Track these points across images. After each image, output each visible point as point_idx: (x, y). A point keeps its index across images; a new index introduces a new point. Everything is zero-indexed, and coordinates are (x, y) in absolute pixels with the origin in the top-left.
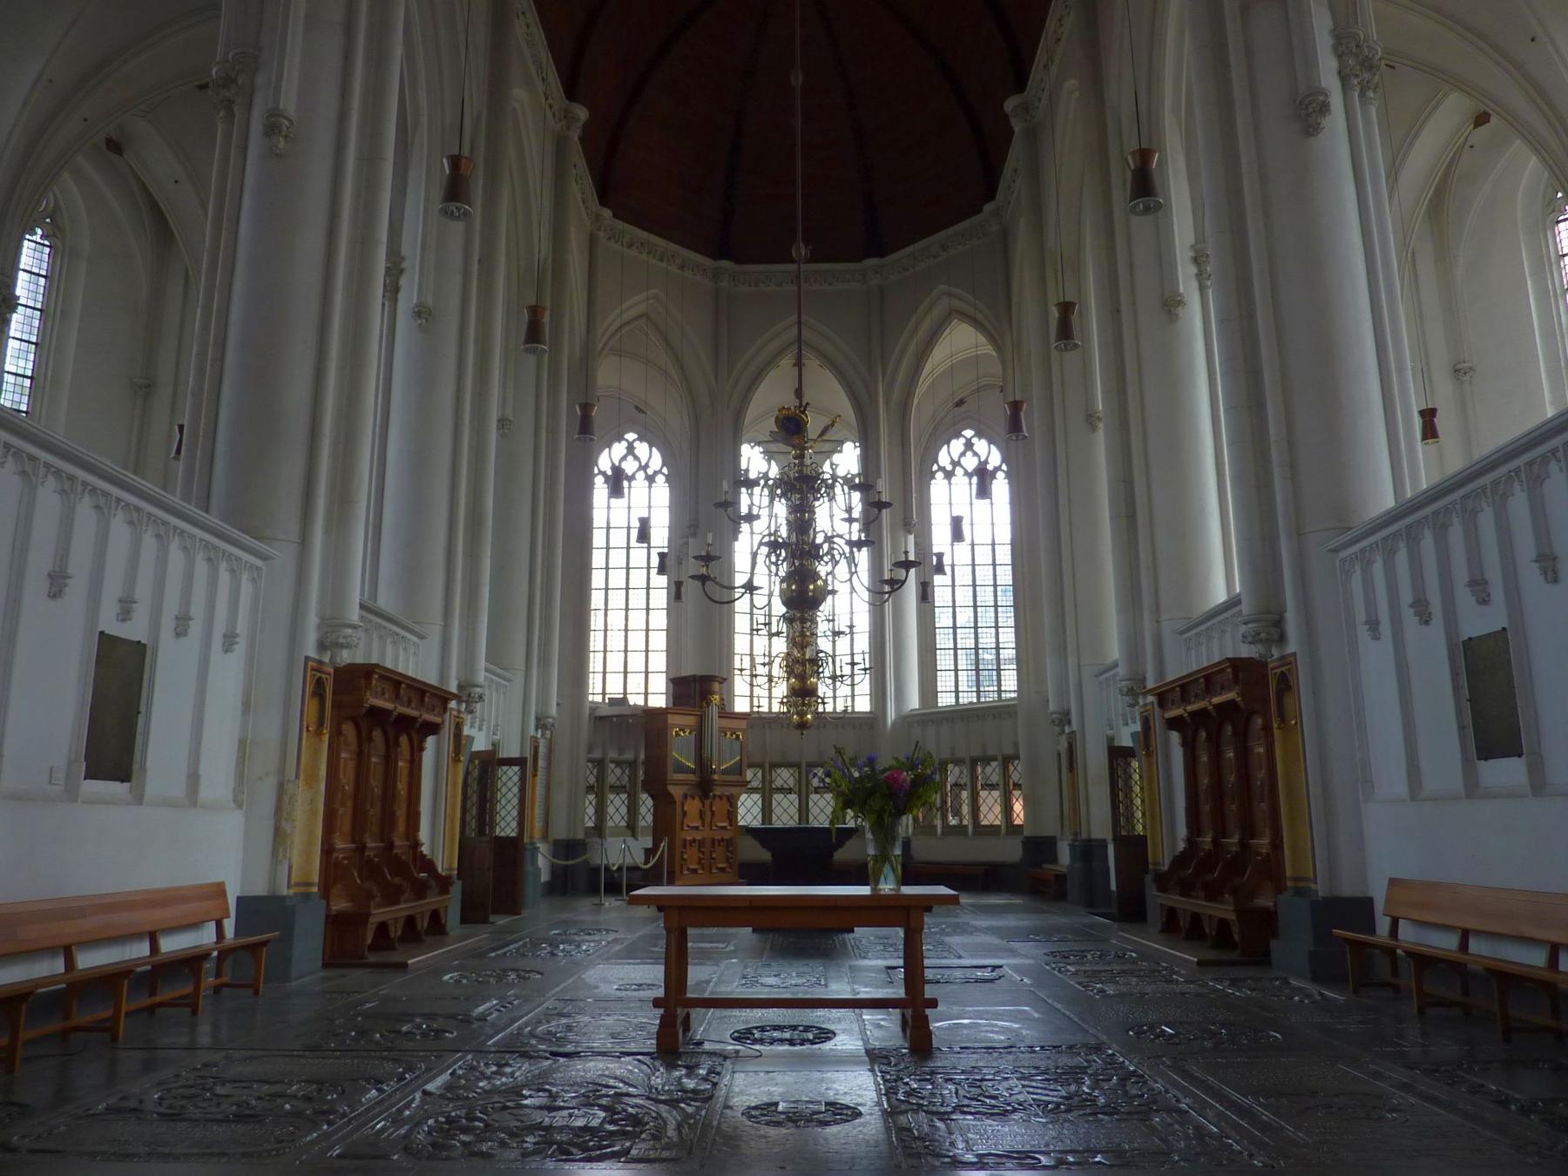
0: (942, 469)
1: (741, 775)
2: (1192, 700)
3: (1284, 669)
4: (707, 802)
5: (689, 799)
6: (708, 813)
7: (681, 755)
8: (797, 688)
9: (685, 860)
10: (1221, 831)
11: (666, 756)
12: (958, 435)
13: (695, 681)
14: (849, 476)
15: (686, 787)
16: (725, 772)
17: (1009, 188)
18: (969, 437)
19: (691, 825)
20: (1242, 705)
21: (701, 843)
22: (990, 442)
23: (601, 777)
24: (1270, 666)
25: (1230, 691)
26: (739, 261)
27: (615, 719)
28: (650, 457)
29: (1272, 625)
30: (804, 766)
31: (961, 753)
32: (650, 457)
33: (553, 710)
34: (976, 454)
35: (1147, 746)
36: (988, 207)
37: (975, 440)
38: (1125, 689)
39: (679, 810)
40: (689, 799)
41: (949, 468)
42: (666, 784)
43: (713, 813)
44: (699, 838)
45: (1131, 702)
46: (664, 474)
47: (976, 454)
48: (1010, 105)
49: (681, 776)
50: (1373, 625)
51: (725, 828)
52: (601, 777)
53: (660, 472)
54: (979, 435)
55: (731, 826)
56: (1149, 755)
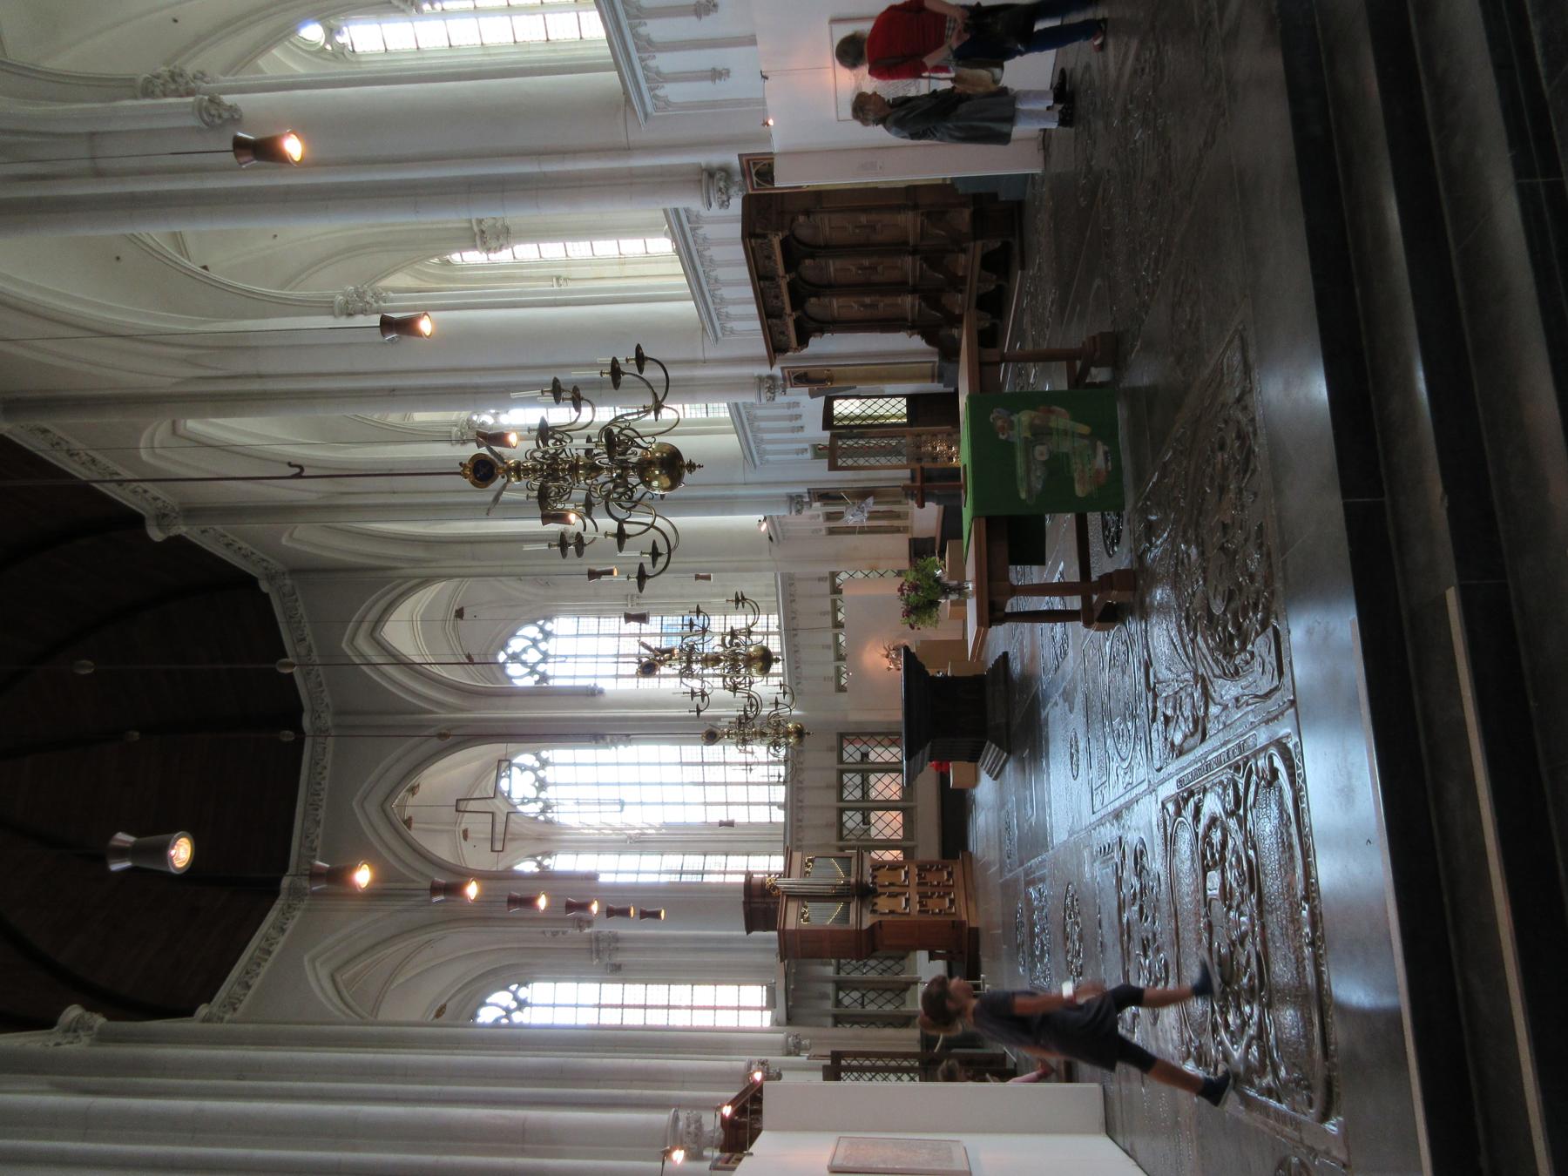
1: (850, 858)
2: (780, 304)
3: (753, 172)
4: (880, 890)
5: (876, 908)
6: (893, 889)
7: (830, 916)
8: (761, 664)
9: (940, 911)
10: (899, 287)
12: (503, 666)
13: (750, 903)
14: (537, 784)
15: (864, 910)
16: (848, 873)
17: (245, 556)
18: (505, 657)
19: (904, 905)
20: (787, 233)
21: (923, 896)
22: (513, 635)
24: (750, 192)
25: (771, 246)
26: (284, 868)
27: (790, 1004)
28: (496, 1005)
29: (711, 179)
30: (842, 805)
32: (496, 1005)
34: (524, 651)
35: (822, 381)
36: (264, 586)
37: (510, 651)
38: (769, 394)
39: (889, 918)
40: (876, 908)
41: (537, 677)
42: (861, 930)
43: (891, 884)
44: (917, 897)
45: (781, 390)
46: (518, 989)
47: (524, 651)
48: (156, 535)
49: (853, 916)
50: (716, 74)
51: (906, 873)
53: (514, 993)
54: (504, 646)
55: (904, 867)
56: (831, 379)
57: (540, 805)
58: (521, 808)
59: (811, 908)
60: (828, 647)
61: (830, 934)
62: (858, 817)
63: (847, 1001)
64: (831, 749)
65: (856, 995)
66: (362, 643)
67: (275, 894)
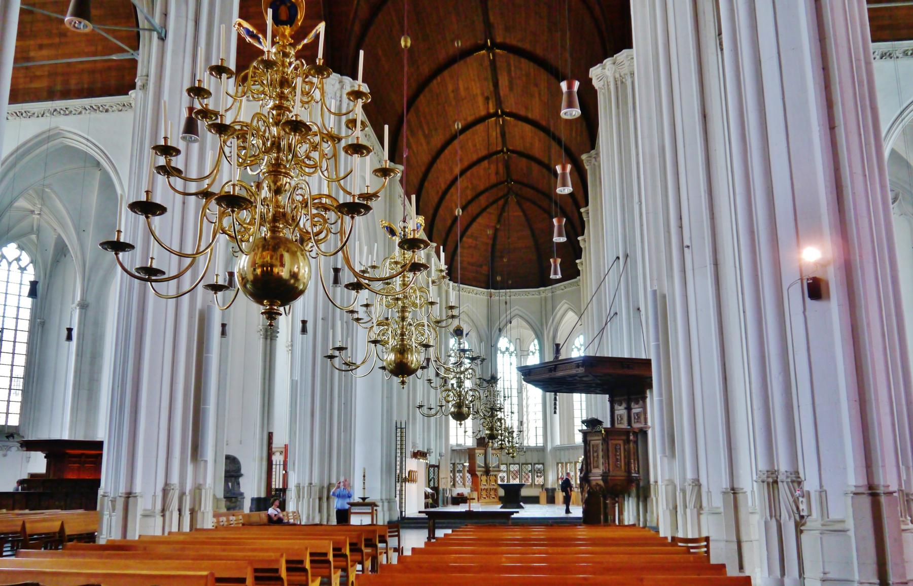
0: (577, 347)
6: (489, 481)
11: (475, 463)
16: (494, 467)
21: (487, 490)
31: (571, 460)
33: (444, 451)
36: (578, 278)
41: (579, 347)
57: (534, 351)
58: (533, 343)
59: (482, 457)
60: (569, 459)
62: (505, 469)
64: (539, 461)
66: (566, 306)
67: (488, 288)
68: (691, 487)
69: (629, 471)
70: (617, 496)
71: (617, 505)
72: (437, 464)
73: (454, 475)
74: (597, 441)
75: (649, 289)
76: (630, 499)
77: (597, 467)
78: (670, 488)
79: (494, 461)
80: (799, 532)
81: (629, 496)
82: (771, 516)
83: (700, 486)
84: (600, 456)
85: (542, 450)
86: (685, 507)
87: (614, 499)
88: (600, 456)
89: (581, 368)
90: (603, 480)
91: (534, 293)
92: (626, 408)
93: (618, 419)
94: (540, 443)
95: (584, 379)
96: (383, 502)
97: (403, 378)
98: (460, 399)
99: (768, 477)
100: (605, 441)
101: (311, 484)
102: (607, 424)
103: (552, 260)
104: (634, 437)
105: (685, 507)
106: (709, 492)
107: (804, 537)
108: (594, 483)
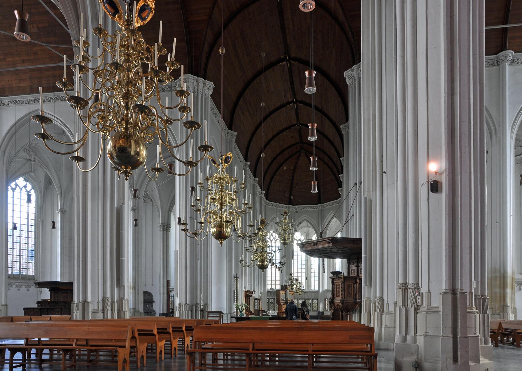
23: (269, 301)
49: (283, 301)
52: (269, 301)
58: (314, 236)
59: (284, 295)
61: (280, 298)
63: (272, 300)
64: (315, 297)
65: (273, 301)
67: (289, 205)
68: (378, 301)
69: (356, 299)
70: (349, 311)
71: (348, 315)
72: (259, 298)
73: (269, 304)
74: (339, 283)
75: (363, 196)
76: (356, 313)
77: (339, 296)
78: (368, 301)
79: (290, 297)
80: (416, 313)
81: (356, 312)
82: (403, 306)
83: (383, 300)
84: (340, 291)
85: (317, 292)
86: (375, 311)
87: (347, 312)
88: (340, 291)
89: (330, 244)
90: (341, 302)
91: (315, 207)
92: (356, 266)
93: (352, 272)
94: (317, 288)
95: (333, 250)
96: (227, 315)
97: (221, 240)
98: (263, 258)
99: (402, 286)
100: (343, 283)
101: (186, 303)
102: (345, 274)
103: (312, 182)
104: (359, 281)
105: (375, 311)
106: (388, 303)
107: (418, 316)
108: (336, 304)
